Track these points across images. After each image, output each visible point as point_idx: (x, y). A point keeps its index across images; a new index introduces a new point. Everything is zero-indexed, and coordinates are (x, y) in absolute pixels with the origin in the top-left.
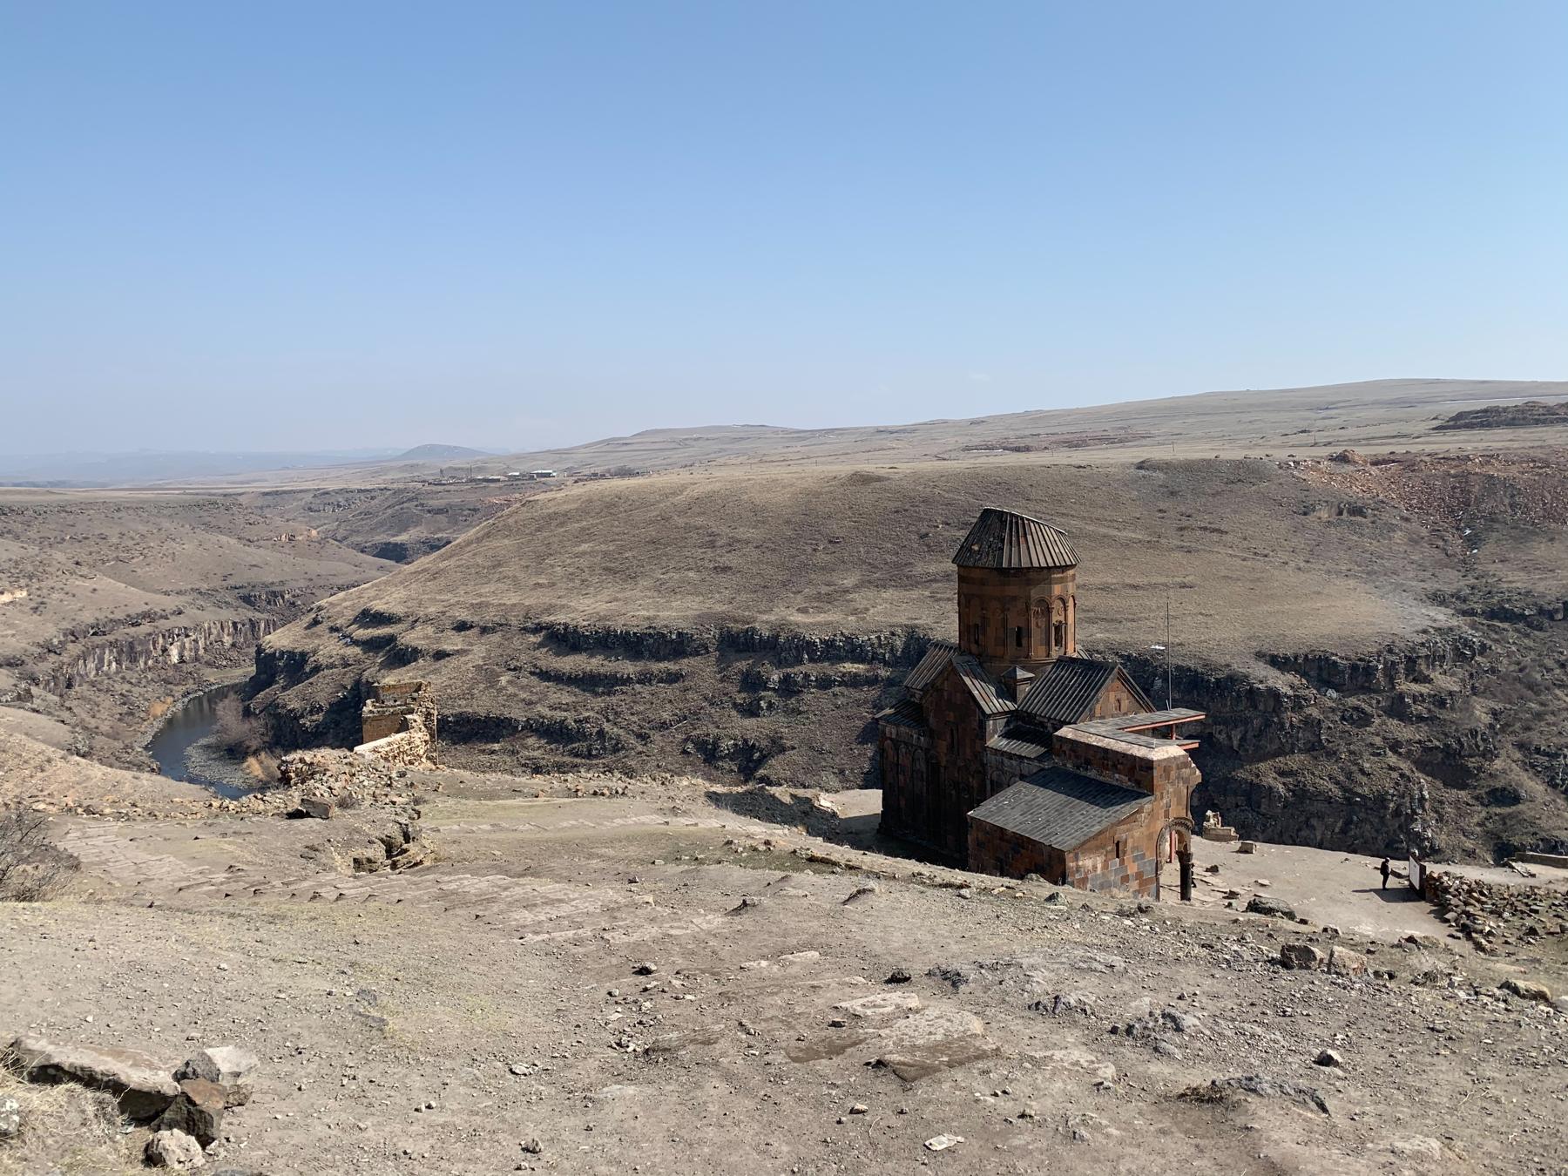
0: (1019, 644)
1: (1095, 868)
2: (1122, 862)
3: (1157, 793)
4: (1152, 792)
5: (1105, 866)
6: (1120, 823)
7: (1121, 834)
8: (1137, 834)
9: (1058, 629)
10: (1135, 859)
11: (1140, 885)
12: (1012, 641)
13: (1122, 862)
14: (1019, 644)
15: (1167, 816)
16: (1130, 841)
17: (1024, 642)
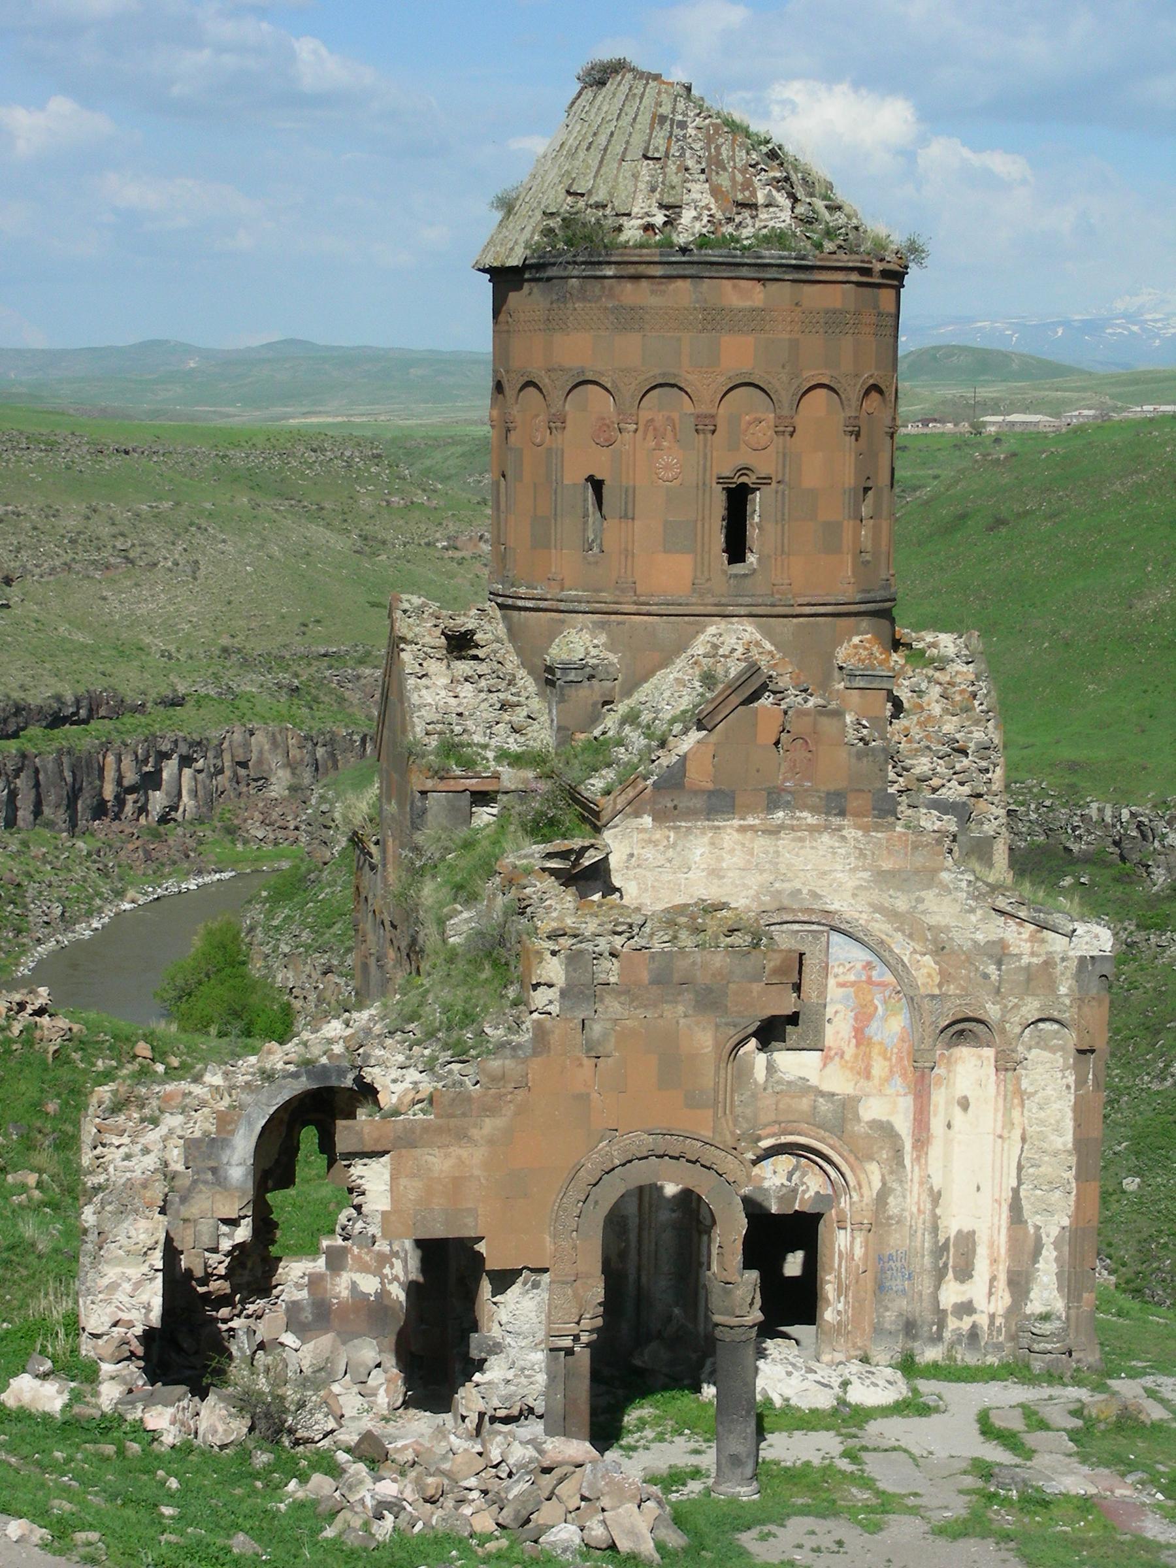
9: (738, 499)
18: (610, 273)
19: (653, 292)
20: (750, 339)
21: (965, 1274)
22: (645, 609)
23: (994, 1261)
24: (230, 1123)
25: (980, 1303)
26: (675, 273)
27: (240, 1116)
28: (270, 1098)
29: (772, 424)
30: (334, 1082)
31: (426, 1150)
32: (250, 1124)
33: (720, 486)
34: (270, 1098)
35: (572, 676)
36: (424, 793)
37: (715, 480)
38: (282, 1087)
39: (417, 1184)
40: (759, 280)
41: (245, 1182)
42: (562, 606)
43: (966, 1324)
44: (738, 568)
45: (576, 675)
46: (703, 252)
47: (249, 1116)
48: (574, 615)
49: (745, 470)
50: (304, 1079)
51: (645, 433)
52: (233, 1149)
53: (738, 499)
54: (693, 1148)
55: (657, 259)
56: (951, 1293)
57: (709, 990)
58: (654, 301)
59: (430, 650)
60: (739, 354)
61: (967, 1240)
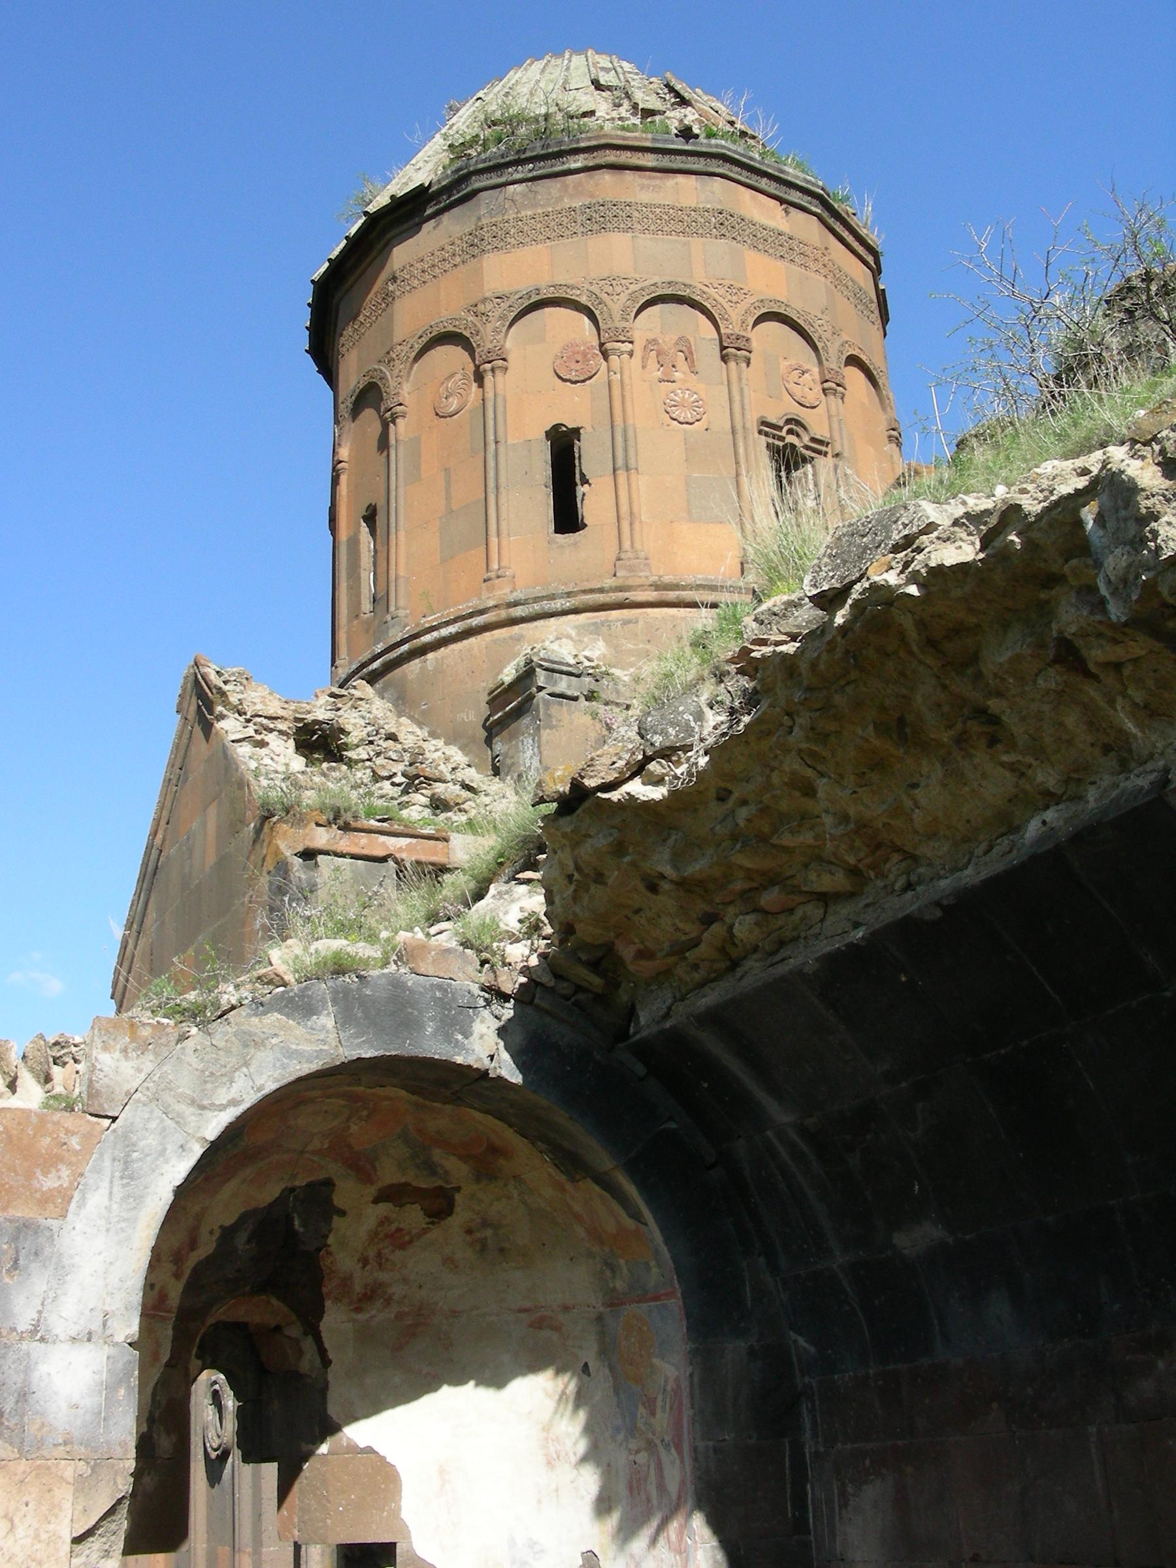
18: (579, 165)
19: (642, 187)
22: (671, 595)
24: (50, 1162)
26: (675, 166)
27: (91, 1142)
28: (209, 1078)
29: (817, 377)
30: (430, 1045)
32: (128, 1172)
33: (763, 440)
34: (209, 1078)
35: (563, 685)
36: (309, 855)
37: (753, 426)
38: (250, 1042)
40: (782, 201)
41: (103, 1416)
42: (518, 612)
45: (569, 687)
46: (713, 141)
47: (127, 1143)
48: (541, 623)
50: (326, 1021)
51: (644, 360)
52: (61, 1272)
55: (648, 144)
58: (645, 197)
59: (265, 721)
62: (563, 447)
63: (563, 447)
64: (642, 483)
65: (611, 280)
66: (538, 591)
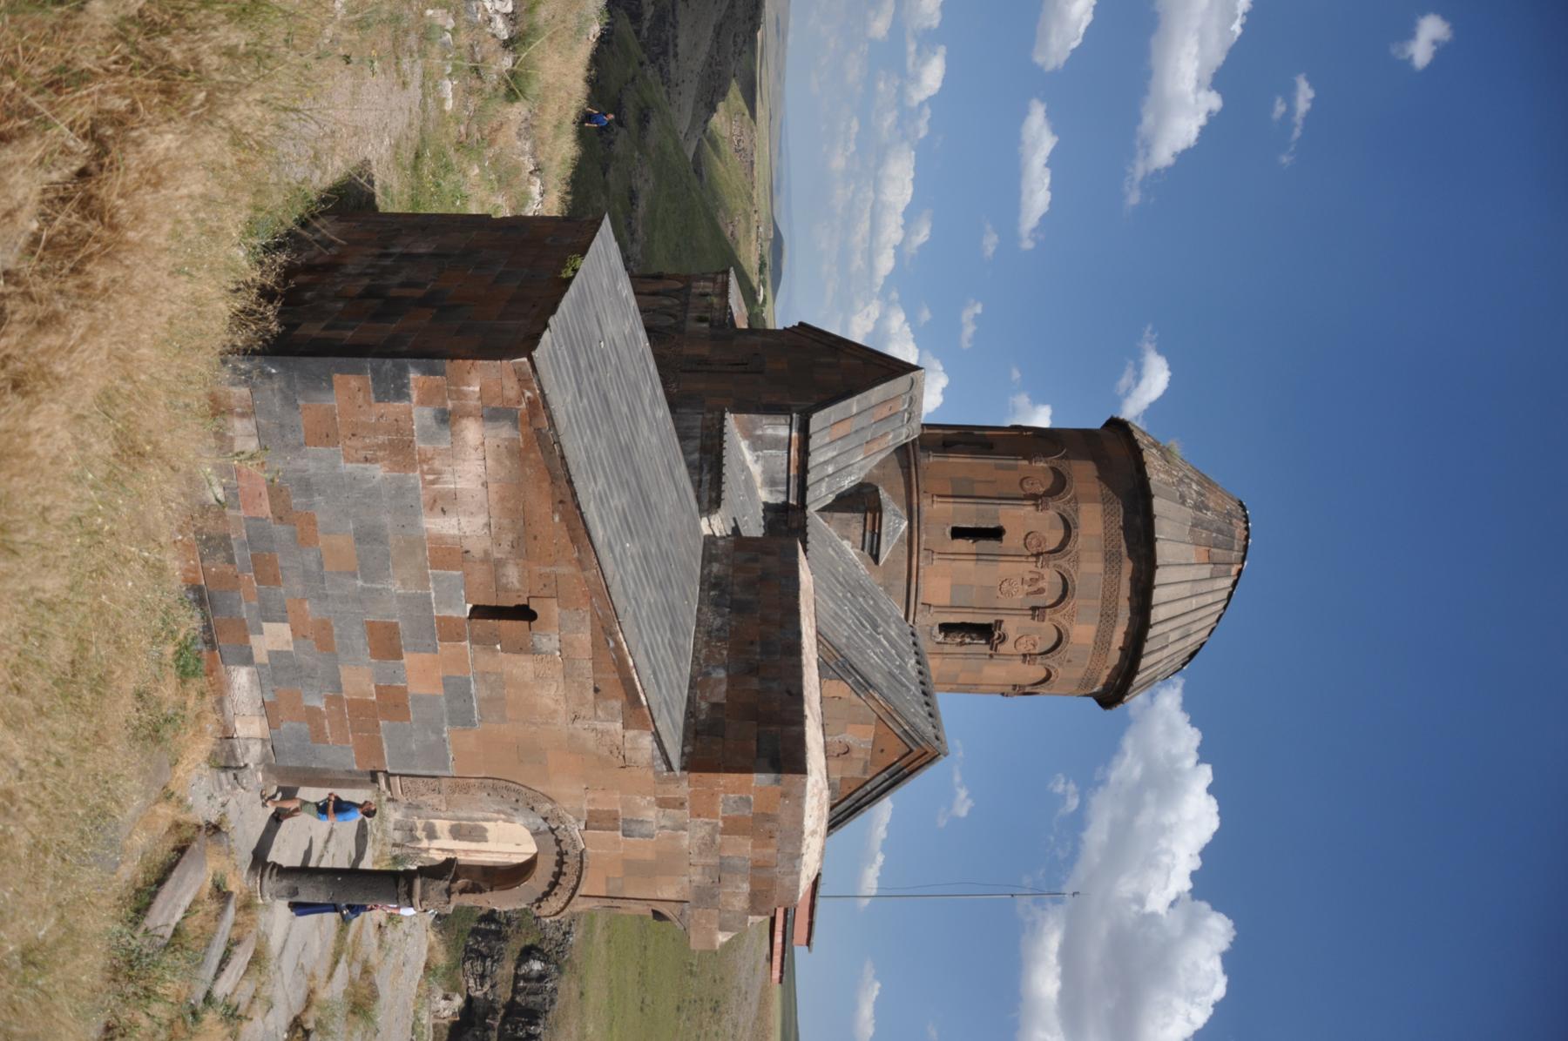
0: (958, 533)
1: (444, 503)
2: (449, 631)
3: (684, 786)
4: (696, 762)
5: (449, 555)
6: (606, 627)
7: (563, 632)
8: (551, 695)
9: (985, 632)
10: (457, 690)
11: (360, 708)
12: (969, 515)
13: (449, 631)
14: (958, 533)
15: (595, 821)
16: (522, 667)
17: (964, 545)
20: (1091, 642)
21: (457, 833)
23: (466, 852)
25: (436, 844)
31: (562, 686)
39: (529, 676)
43: (420, 834)
44: (936, 629)
49: (1003, 639)
53: (985, 632)
54: (567, 882)
56: (442, 826)
57: (714, 896)
60: (1083, 633)
61: (477, 834)
62: (996, 534)
63: (996, 534)
64: (972, 564)
65: (1077, 561)
66: (923, 516)
